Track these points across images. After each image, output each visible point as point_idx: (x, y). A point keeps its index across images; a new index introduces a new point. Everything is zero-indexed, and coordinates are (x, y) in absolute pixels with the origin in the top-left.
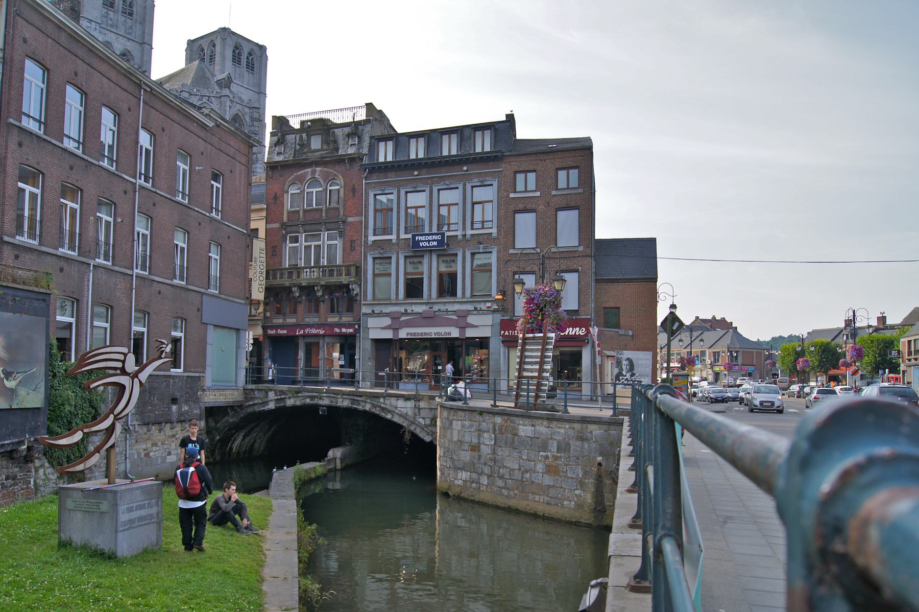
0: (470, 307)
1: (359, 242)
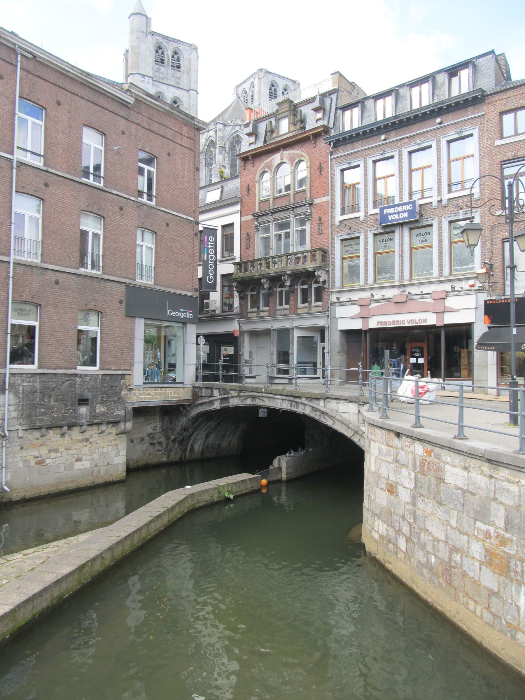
0: (447, 287)
1: (326, 224)
